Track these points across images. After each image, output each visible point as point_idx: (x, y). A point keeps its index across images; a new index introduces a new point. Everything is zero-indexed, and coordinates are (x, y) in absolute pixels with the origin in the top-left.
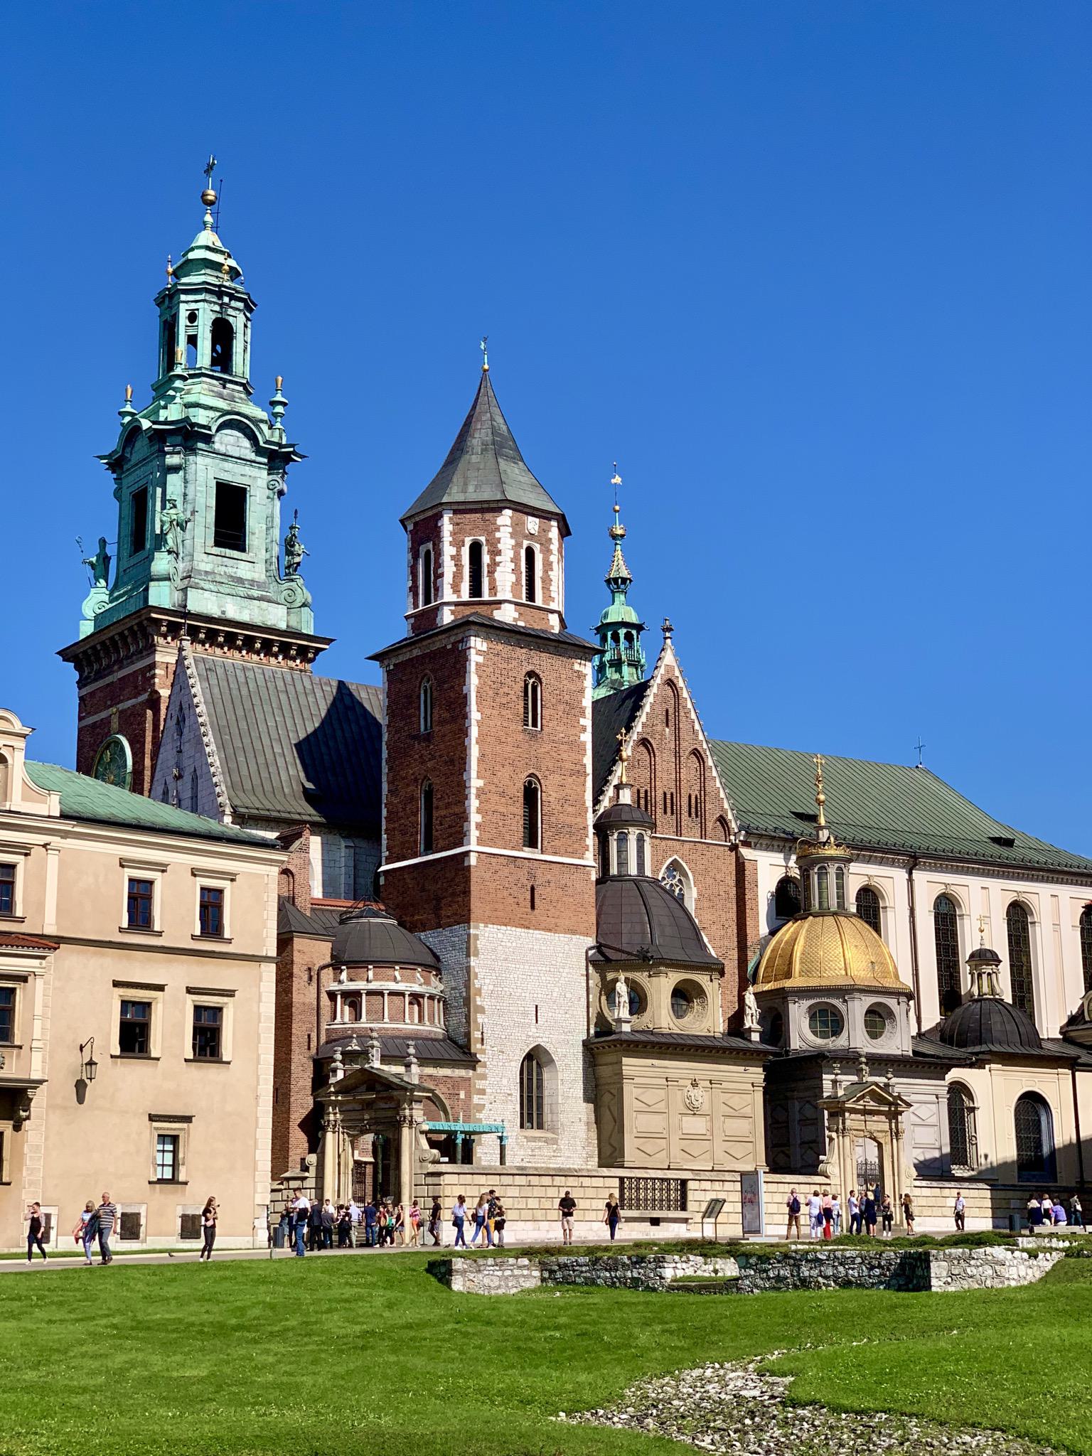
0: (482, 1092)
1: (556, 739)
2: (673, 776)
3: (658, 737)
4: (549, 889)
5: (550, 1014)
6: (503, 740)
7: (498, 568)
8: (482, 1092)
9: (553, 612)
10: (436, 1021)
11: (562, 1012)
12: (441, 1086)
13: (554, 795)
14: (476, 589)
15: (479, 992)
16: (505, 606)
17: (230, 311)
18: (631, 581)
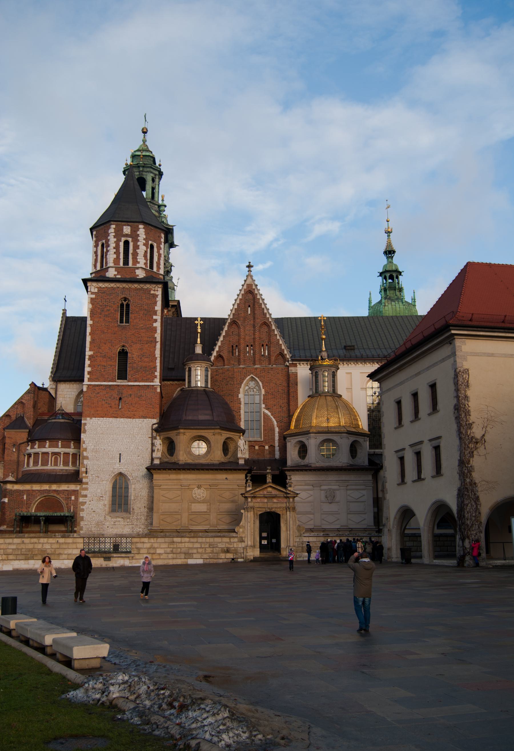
0: (86, 496)
1: (137, 327)
2: (252, 337)
3: (242, 319)
4: (130, 399)
5: (128, 457)
6: (106, 331)
7: (108, 253)
8: (86, 496)
9: (138, 268)
10: (70, 464)
11: (135, 456)
12: (61, 494)
13: (136, 354)
14: (102, 266)
15: (86, 450)
16: (110, 269)
17: (144, 173)
18: (394, 252)
